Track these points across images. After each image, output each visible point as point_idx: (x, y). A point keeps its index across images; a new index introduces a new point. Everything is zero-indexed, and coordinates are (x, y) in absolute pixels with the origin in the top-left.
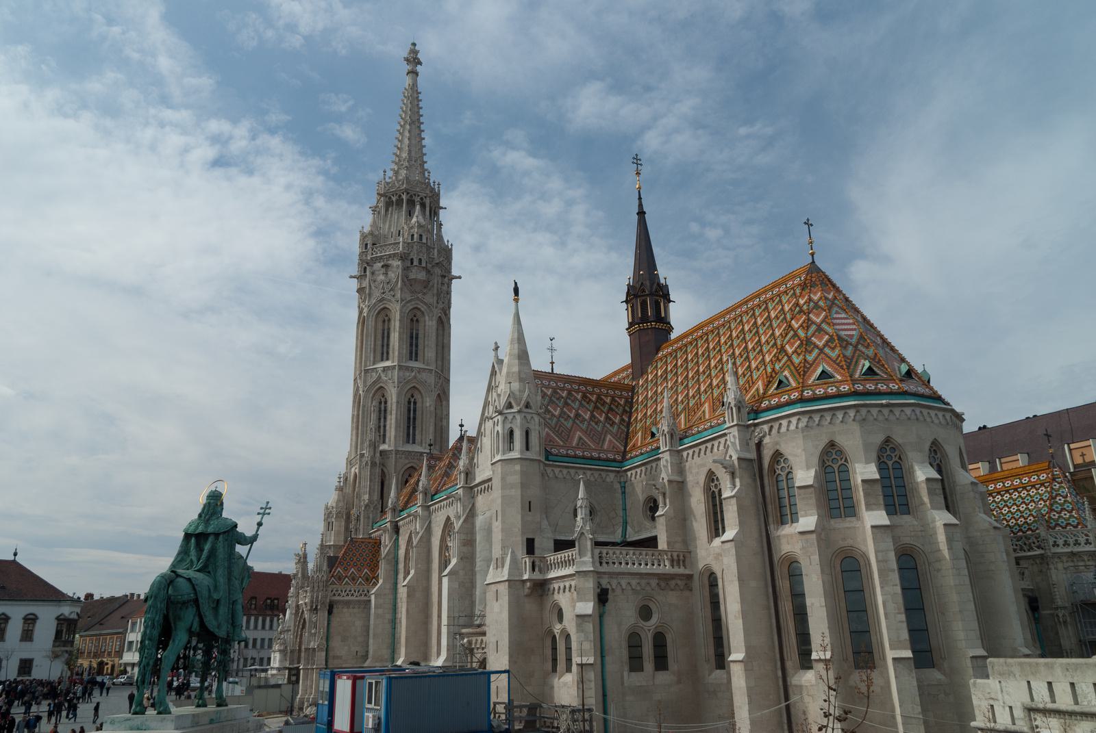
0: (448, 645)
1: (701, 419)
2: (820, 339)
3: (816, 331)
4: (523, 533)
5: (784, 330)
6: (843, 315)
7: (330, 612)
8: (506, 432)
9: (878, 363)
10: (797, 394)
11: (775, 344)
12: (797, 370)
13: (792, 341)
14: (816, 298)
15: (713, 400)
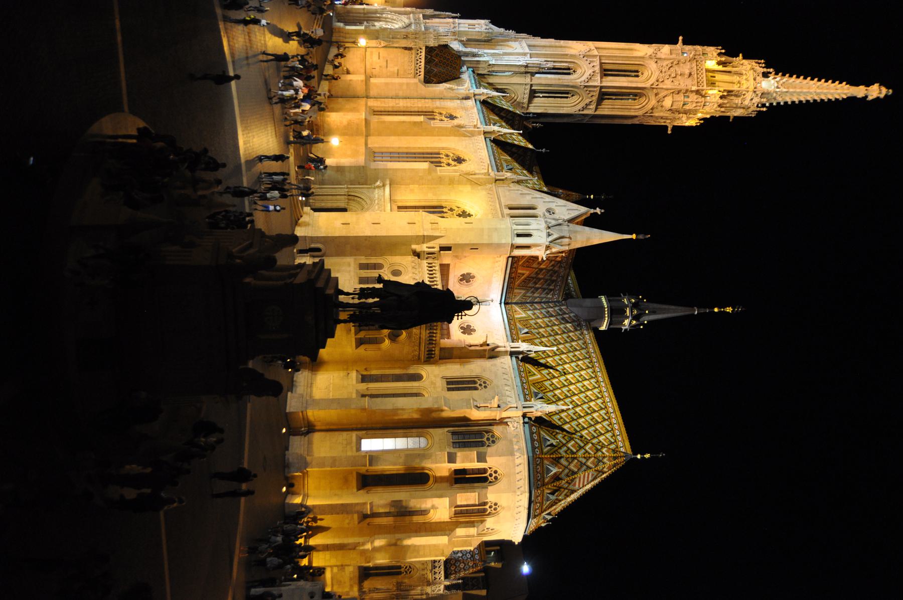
0: (378, 169)
1: (530, 373)
2: (575, 466)
3: (580, 462)
4: (455, 244)
5: (586, 438)
6: (590, 479)
7: (406, 48)
8: (531, 231)
9: (554, 502)
10: (538, 453)
11: (577, 431)
12: (555, 452)
13: (577, 445)
14: (605, 460)
15: (542, 382)
